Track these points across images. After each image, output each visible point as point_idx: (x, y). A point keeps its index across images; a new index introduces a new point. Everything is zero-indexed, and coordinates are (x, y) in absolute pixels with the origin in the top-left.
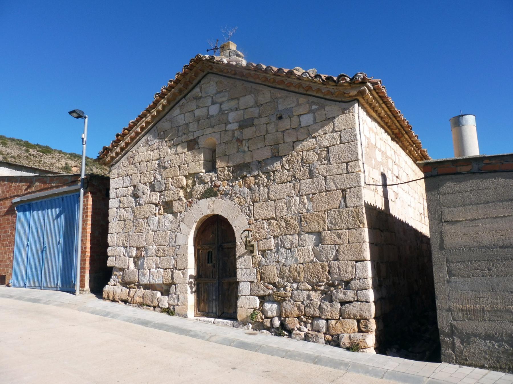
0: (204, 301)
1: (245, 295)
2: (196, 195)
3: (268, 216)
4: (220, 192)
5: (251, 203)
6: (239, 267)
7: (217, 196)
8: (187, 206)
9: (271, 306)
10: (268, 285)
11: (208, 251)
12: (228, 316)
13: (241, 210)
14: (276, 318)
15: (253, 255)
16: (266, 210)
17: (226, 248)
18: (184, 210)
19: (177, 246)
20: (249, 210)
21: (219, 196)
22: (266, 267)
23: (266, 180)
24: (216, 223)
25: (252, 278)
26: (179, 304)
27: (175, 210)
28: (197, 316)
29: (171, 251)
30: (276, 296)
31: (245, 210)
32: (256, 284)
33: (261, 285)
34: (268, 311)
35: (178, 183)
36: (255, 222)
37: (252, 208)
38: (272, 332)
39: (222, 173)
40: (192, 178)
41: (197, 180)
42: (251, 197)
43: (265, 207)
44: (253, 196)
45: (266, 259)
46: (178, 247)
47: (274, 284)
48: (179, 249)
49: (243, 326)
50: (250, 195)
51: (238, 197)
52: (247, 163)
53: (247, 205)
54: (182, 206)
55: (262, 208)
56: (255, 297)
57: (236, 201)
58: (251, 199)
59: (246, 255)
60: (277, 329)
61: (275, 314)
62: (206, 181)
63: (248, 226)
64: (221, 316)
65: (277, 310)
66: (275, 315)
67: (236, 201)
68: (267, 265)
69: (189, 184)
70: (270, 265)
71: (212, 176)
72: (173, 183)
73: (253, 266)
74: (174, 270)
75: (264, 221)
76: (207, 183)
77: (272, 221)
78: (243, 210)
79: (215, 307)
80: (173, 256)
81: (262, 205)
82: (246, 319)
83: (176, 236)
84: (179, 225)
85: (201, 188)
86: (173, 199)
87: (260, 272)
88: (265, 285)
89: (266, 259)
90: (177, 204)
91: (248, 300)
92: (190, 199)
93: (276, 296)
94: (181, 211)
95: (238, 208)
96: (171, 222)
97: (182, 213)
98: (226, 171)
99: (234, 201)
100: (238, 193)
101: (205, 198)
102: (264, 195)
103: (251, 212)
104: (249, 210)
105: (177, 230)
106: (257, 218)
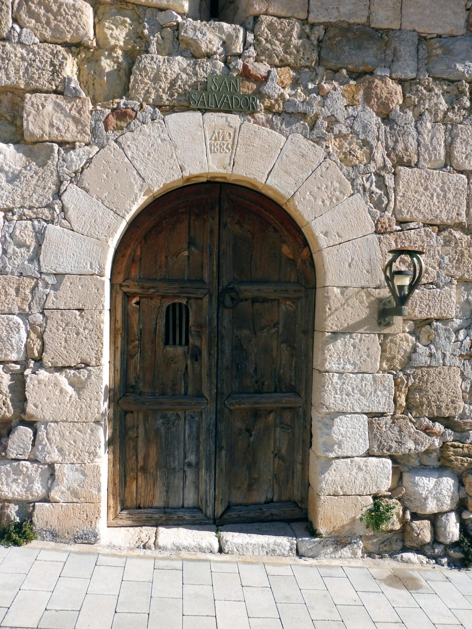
0: (144, 469)
1: (349, 454)
2: (153, 91)
3: (444, 216)
4: (267, 102)
5: (389, 164)
6: (335, 367)
7: (252, 114)
8: (101, 125)
9: (437, 484)
10: (431, 423)
11: (168, 303)
12: (252, 515)
13: (352, 181)
14: (453, 517)
15: (386, 331)
16: (438, 195)
17: (246, 300)
18: (87, 139)
19: (48, 274)
20: (381, 183)
21: (261, 116)
22: (432, 370)
23: (444, 106)
24: (217, 209)
25: (379, 403)
26: (57, 498)
27: (37, 132)
28: (120, 522)
29: (12, 292)
30: (456, 454)
31: (367, 185)
32: (390, 422)
33: (410, 424)
34: (426, 499)
35: (53, 23)
36: (399, 228)
37: (390, 181)
38: (436, 558)
39: (275, 35)
40: (128, 20)
41: (152, 33)
42: (391, 144)
43: (435, 184)
44: (396, 142)
45: (432, 347)
46: (51, 280)
47: (448, 422)
48: (55, 288)
49: (336, 550)
50: (386, 138)
51: (340, 136)
52: (377, 30)
53: (372, 168)
54: (77, 121)
55: (426, 189)
56: (384, 459)
57: (333, 145)
58: (390, 151)
59: (362, 330)
60: (456, 545)
61: (447, 503)
62: (204, 48)
63: (375, 237)
64: (226, 516)
65: (453, 493)
66: (446, 508)
67: (333, 145)
68: (434, 363)
69: (113, 42)
70: (444, 365)
71: (229, 36)
72: (24, 16)
73: (385, 366)
74: (25, 366)
75: (429, 229)
76: (209, 56)
77: (458, 234)
78: (359, 181)
79: (192, 490)
80: (24, 315)
81: (426, 179)
82: (347, 528)
83: (40, 236)
84: (58, 195)
85: (176, 69)
86: (27, 84)
87: (410, 384)
88: (421, 425)
89: (432, 347)
90: (49, 107)
91: (362, 470)
92: (122, 101)
93: (456, 454)
94: (68, 137)
95: (341, 173)
96: (13, 178)
97: (74, 148)
98: (295, 34)
99: (324, 143)
100: (342, 120)
101: (194, 110)
102: (435, 149)
103: (387, 195)
104: (381, 183)
105: (46, 211)
106: (408, 217)
